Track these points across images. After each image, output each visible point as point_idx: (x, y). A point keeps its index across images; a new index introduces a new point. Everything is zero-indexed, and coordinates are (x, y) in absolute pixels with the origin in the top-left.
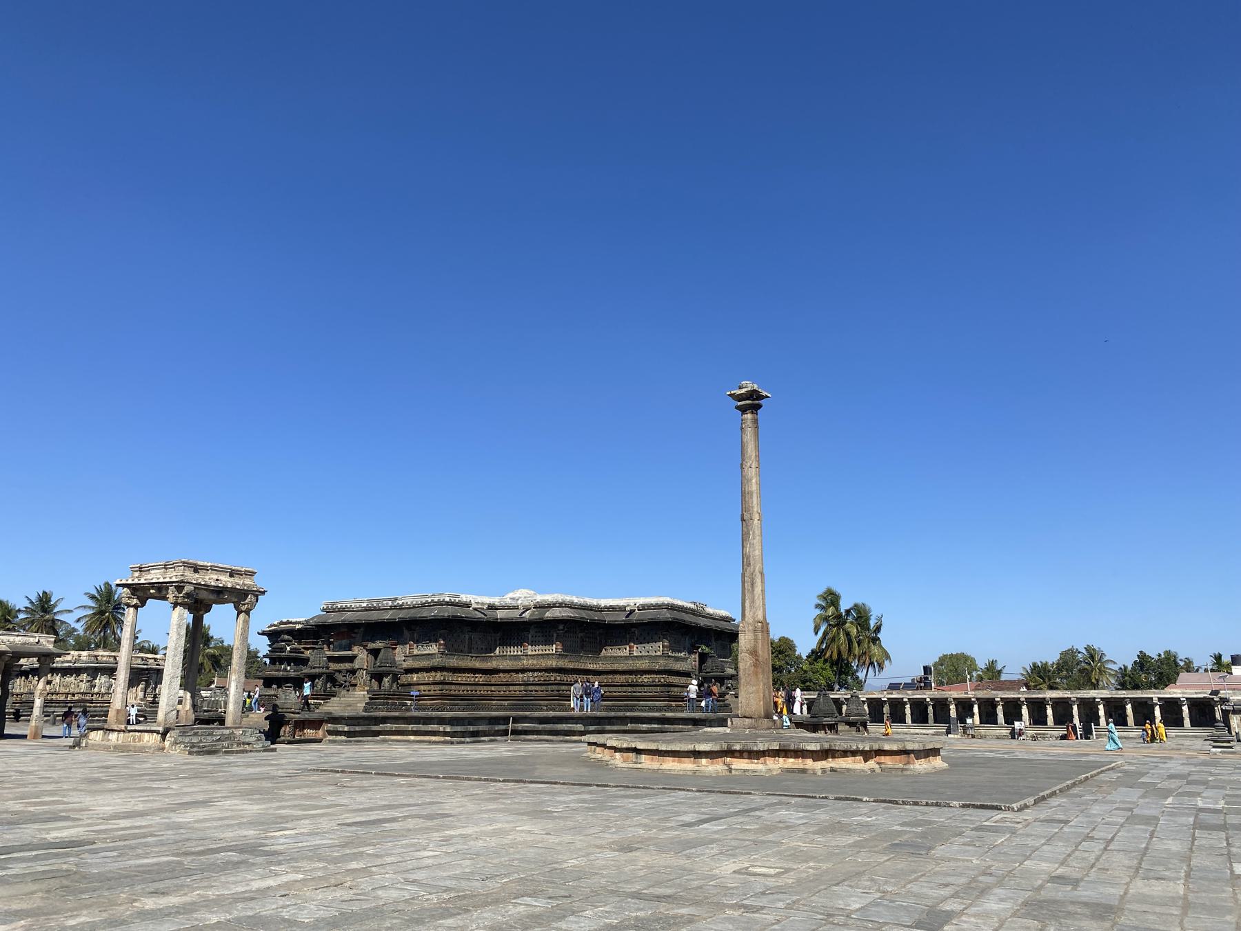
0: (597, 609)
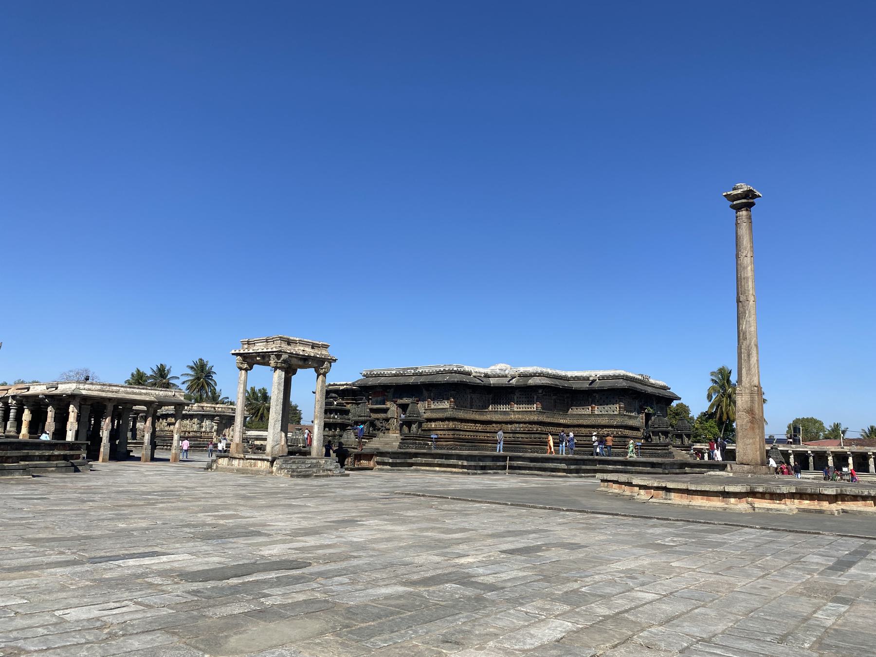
0: (565, 378)
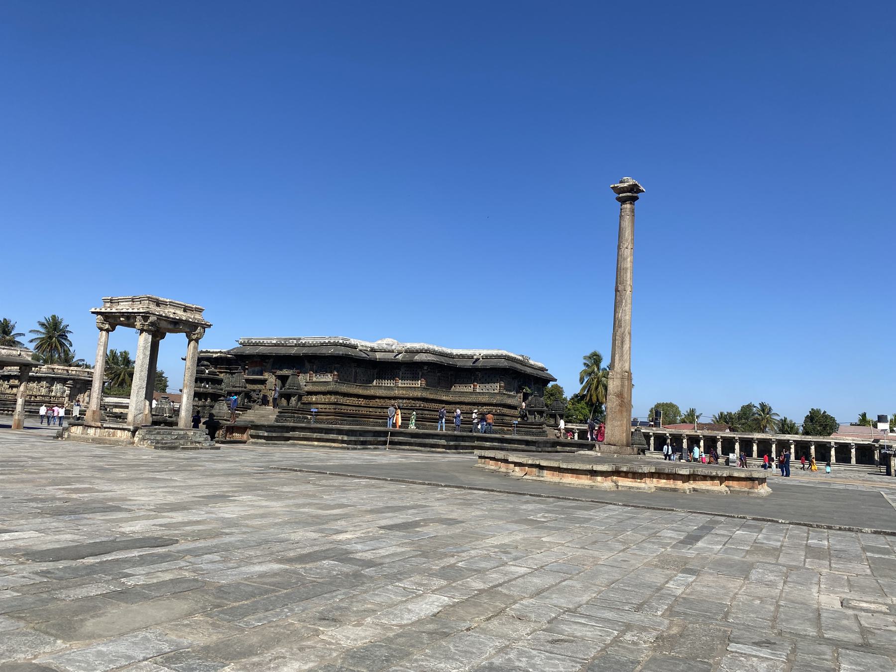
0: (450, 356)
